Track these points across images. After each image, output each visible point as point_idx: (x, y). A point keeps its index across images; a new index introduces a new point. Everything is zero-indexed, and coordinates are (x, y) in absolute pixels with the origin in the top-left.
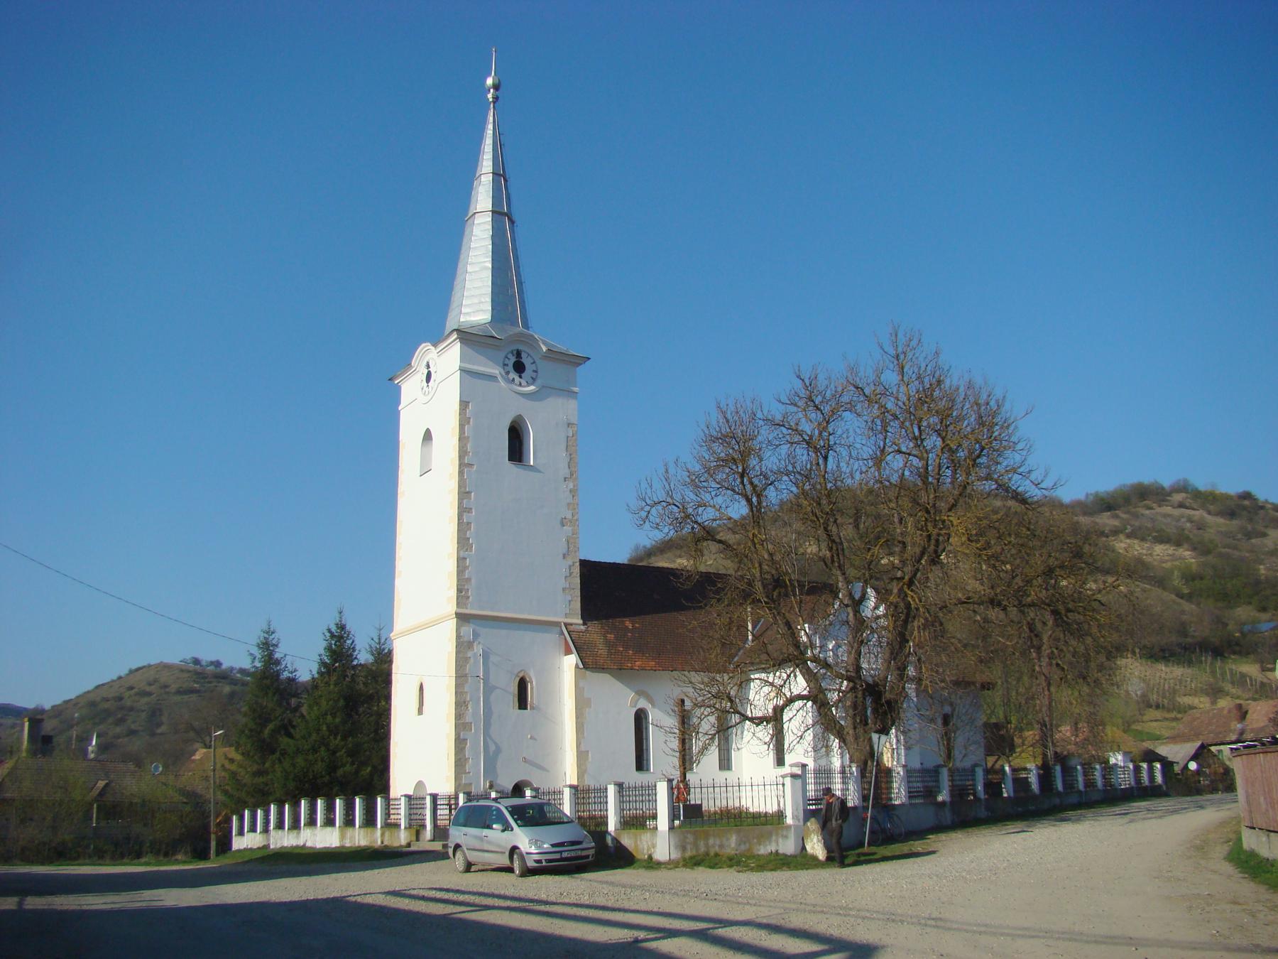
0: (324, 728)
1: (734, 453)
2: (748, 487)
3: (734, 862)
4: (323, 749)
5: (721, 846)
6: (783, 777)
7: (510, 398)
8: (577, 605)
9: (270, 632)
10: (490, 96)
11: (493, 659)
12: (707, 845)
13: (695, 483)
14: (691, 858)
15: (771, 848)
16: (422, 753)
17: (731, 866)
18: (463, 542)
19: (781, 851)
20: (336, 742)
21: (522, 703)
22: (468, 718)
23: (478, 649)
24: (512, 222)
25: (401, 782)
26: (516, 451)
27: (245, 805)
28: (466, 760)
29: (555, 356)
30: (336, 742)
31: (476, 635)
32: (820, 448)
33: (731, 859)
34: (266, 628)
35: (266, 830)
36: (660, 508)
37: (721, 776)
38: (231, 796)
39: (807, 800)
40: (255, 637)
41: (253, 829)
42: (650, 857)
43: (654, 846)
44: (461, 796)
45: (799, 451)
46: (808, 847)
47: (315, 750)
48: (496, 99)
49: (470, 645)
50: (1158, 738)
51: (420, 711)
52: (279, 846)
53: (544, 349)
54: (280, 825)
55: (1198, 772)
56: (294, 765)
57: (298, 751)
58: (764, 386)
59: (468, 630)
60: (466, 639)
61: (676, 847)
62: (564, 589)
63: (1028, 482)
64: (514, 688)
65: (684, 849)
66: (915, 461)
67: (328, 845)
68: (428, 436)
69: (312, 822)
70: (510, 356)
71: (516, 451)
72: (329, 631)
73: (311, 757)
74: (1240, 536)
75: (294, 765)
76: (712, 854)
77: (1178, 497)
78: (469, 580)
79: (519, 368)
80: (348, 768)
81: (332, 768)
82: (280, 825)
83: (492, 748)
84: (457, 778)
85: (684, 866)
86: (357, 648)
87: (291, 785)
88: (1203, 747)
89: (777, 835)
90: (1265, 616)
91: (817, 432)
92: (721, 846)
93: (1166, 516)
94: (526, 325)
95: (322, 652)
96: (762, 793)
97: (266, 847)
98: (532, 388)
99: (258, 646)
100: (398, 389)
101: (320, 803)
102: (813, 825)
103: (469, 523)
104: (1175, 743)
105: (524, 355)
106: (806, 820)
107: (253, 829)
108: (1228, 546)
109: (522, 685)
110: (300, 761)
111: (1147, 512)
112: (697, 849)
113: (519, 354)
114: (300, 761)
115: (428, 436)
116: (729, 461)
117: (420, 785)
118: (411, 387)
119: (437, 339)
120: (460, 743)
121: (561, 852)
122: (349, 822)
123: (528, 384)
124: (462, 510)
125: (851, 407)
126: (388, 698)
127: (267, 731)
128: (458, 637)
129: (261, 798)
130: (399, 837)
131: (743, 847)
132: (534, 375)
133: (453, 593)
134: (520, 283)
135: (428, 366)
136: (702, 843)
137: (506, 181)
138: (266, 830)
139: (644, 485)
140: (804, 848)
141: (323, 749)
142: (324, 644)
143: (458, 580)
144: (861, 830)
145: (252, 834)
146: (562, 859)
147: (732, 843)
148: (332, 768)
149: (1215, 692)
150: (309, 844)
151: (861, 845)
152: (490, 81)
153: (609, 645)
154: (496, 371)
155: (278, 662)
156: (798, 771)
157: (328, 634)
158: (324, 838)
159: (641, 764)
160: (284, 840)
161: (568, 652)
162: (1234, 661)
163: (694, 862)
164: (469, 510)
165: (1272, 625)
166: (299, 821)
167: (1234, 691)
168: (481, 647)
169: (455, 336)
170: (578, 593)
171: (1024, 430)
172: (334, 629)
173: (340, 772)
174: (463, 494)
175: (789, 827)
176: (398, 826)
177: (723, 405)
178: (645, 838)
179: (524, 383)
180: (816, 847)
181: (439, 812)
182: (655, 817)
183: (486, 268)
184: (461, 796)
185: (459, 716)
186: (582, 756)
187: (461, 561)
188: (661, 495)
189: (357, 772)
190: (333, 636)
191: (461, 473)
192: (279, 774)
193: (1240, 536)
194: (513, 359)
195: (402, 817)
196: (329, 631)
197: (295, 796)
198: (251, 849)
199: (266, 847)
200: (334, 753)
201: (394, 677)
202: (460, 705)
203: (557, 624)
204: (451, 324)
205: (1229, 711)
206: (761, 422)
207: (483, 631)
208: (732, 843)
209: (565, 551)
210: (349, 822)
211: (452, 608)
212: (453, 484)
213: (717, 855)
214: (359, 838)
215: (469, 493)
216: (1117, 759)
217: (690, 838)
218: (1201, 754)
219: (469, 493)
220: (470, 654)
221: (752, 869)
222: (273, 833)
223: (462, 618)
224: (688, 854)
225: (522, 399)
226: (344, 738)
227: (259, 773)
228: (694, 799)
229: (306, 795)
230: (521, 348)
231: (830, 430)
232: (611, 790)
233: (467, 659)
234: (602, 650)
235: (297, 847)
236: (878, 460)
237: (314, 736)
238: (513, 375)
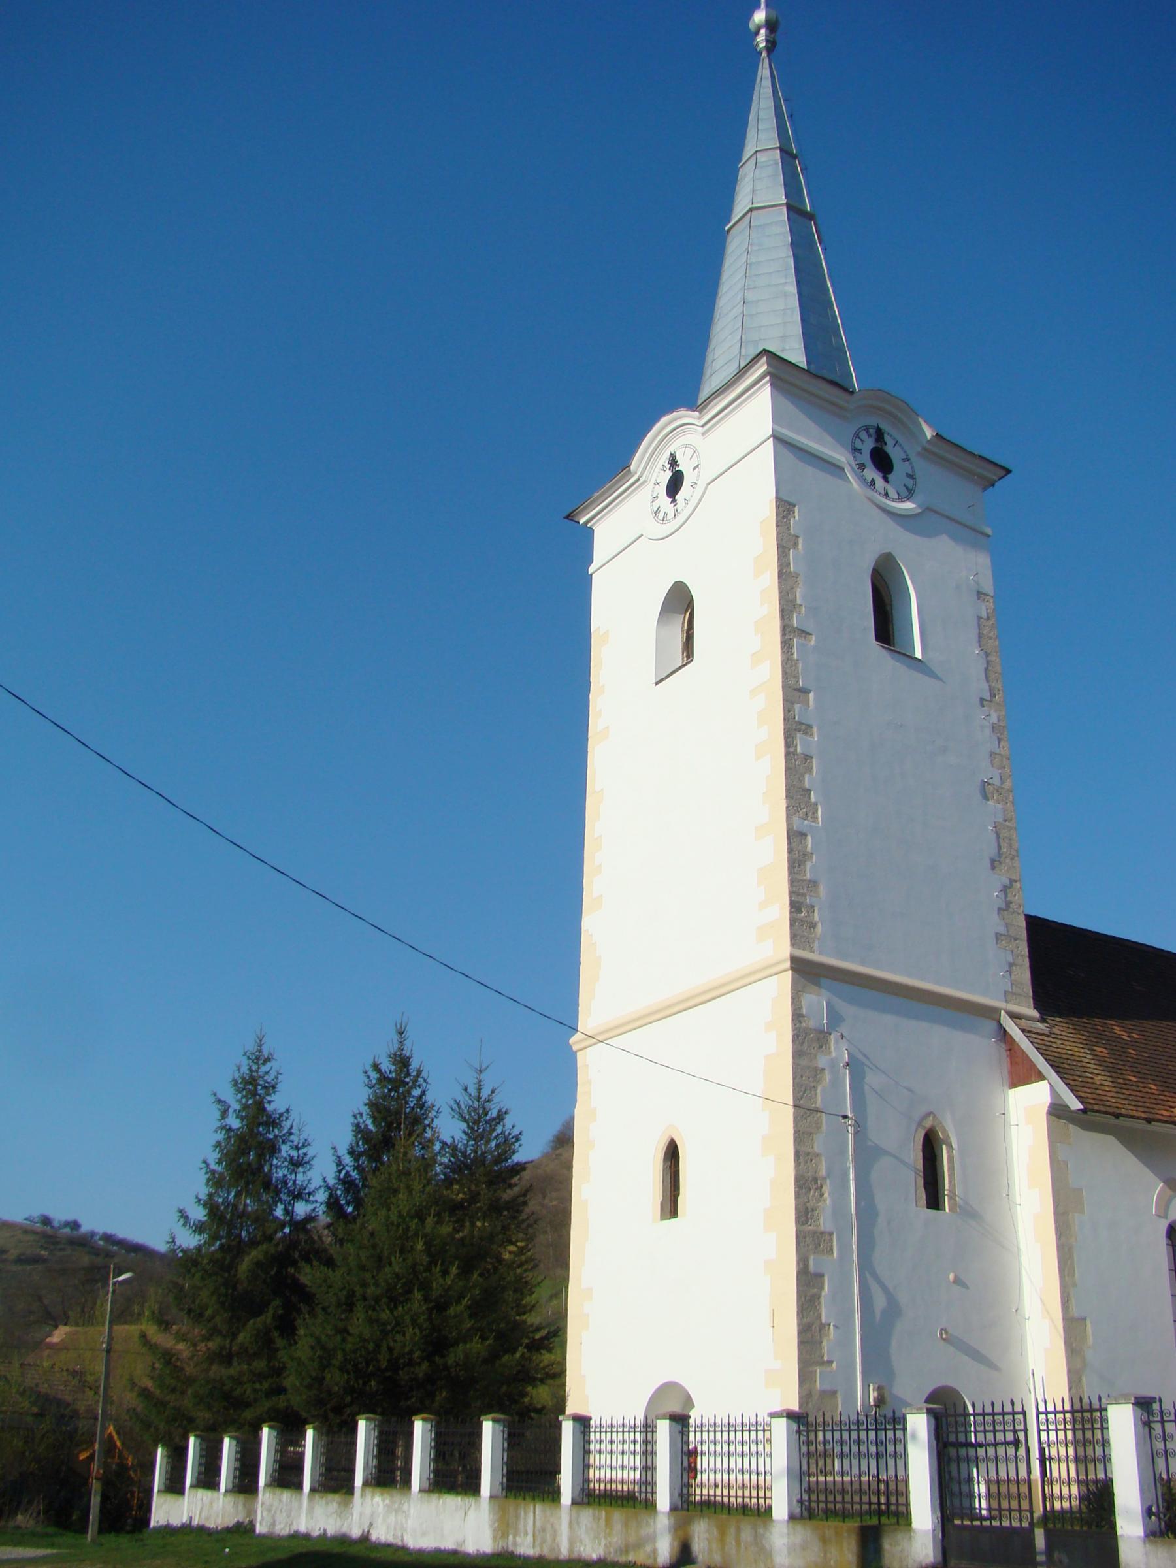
0: (420, 1246)
4: (417, 1295)
7: (869, 520)
8: (1024, 975)
11: (872, 1079)
22: (825, 1222)
23: (839, 1051)
26: (886, 626)
27: (187, 1424)
28: (823, 1327)
29: (947, 451)
30: (445, 1280)
31: (835, 1018)
34: (251, 1047)
35: (246, 1484)
38: (161, 1405)
40: (221, 1080)
41: (208, 1479)
44: (1122, 1423)
51: (671, 1206)
52: (282, 1529)
53: (929, 433)
59: (818, 1001)
60: (812, 1024)
62: (998, 936)
64: (915, 1156)
67: (448, 1544)
68: (679, 602)
70: (863, 435)
71: (886, 626)
72: (376, 1067)
73: (385, 1315)
78: (813, 884)
79: (882, 462)
80: (476, 1346)
81: (437, 1345)
83: (880, 1302)
84: (805, 1377)
87: (335, 1379)
95: (365, 1110)
97: (243, 1530)
98: (908, 506)
99: (235, 1083)
100: (588, 534)
103: (807, 757)
107: (208, 1479)
113: (879, 435)
114: (359, 1324)
115: (679, 602)
120: (808, 1283)
123: (901, 499)
127: (244, 1267)
129: (231, 1412)
133: (780, 911)
138: (246, 1484)
141: (417, 1295)
143: (792, 882)
145: (204, 1495)
148: (437, 1345)
150: (380, 1534)
153: (1099, 1060)
154: (842, 457)
155: (273, 1122)
157: (374, 1075)
161: (1022, 1074)
164: (807, 729)
168: (844, 1045)
169: (762, 367)
170: (1023, 948)
172: (387, 1066)
173: (456, 1356)
174: (794, 693)
176: (765, 1513)
179: (892, 493)
183: (786, 295)
184: (1122, 1423)
185: (804, 1215)
187: (795, 837)
190: (383, 1079)
191: (786, 646)
194: (869, 444)
196: (376, 1067)
197: (338, 1410)
198: (202, 1529)
199: (243, 1530)
200: (440, 1306)
203: (990, 1013)
207: (847, 1010)
209: (993, 851)
211: (779, 947)
212: (771, 671)
215: (805, 691)
219: (805, 691)
220: (822, 1061)
222: (265, 1495)
223: (806, 972)
225: (890, 523)
226: (466, 1271)
227: (225, 1357)
229: (368, 1409)
230: (884, 426)
233: (817, 1072)
235: (343, 1539)
238: (871, 473)
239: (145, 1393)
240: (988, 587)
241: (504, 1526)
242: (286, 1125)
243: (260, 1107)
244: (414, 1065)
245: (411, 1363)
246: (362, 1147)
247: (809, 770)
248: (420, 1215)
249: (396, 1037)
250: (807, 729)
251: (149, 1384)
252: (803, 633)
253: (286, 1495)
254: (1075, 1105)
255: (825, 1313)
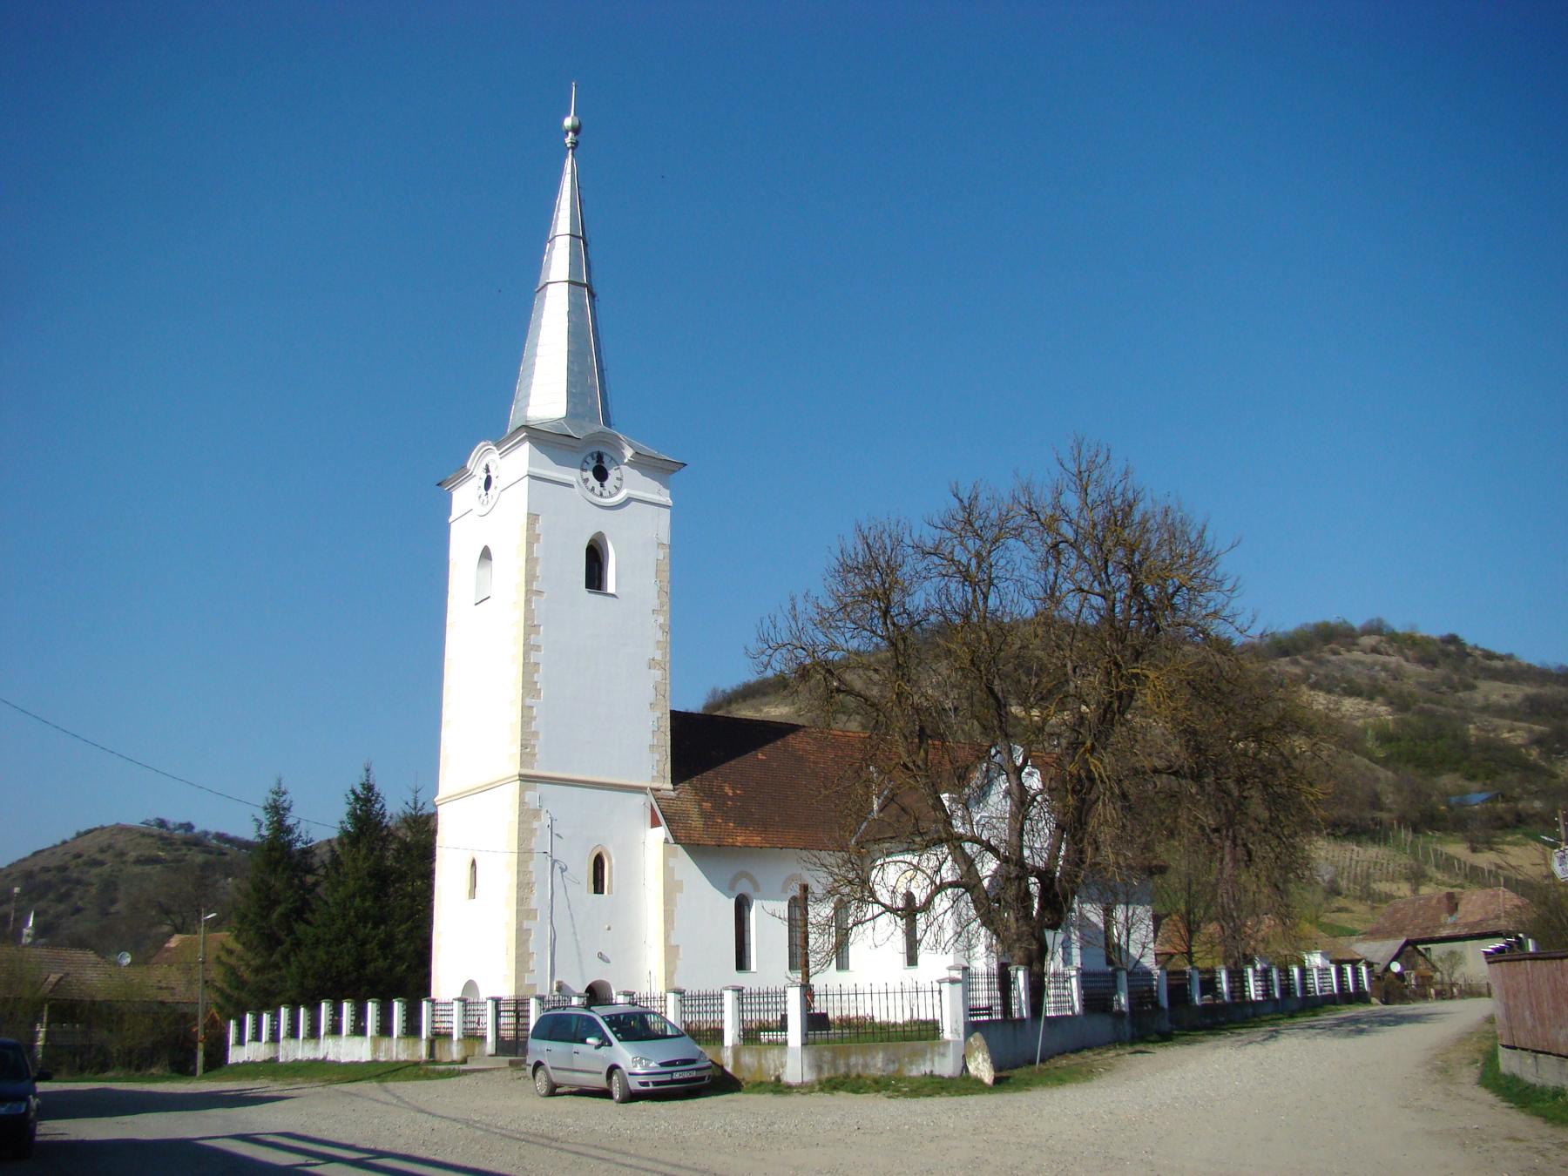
1: (874, 581)
2: (891, 628)
3: (883, 1085)
5: (865, 1066)
6: (940, 982)
9: (279, 793)
10: (568, 140)
12: (848, 1065)
13: (825, 621)
14: (829, 1080)
15: (925, 1068)
16: (475, 947)
17: (878, 1091)
18: (529, 687)
19: (936, 1072)
20: (364, 931)
21: (598, 886)
22: (533, 904)
24: (592, 295)
25: (445, 982)
32: (978, 578)
33: (876, 1081)
34: (274, 787)
35: (274, 1038)
36: (784, 651)
37: (845, 980)
38: (228, 998)
39: (973, 1010)
42: (778, 1079)
43: (783, 1066)
45: (953, 586)
46: (971, 1068)
47: (340, 940)
48: (575, 145)
49: (536, 814)
50: (1352, 933)
52: (291, 1059)
54: (293, 1033)
55: (1400, 976)
56: (313, 958)
57: (318, 942)
58: (911, 503)
59: (535, 793)
61: (810, 1067)
63: (1232, 629)
65: (820, 1069)
66: (1097, 601)
67: (356, 1059)
68: (486, 554)
69: (335, 1029)
70: (589, 459)
72: (354, 792)
73: (333, 949)
74: (1444, 689)
75: (313, 958)
76: (854, 1075)
77: (1368, 641)
80: (381, 963)
81: (361, 963)
82: (293, 1033)
85: (822, 1090)
86: (388, 814)
88: (1407, 943)
89: (933, 1052)
90: (1475, 785)
91: (974, 562)
92: (865, 1066)
93: (1356, 662)
94: (607, 423)
95: (345, 818)
96: (899, 1003)
97: (274, 1060)
101: (347, 1007)
102: (977, 1039)
103: (537, 664)
104: (1375, 939)
105: (606, 459)
106: (968, 1034)
107: (257, 1037)
108: (1432, 701)
109: (598, 863)
110: (321, 954)
111: (1333, 658)
112: (836, 1070)
113: (600, 457)
114: (321, 954)
115: (486, 554)
116: (868, 595)
117: (470, 986)
118: (465, 496)
119: (501, 438)
121: (671, 1073)
122: (385, 1029)
124: (529, 648)
125: (1018, 533)
126: (428, 876)
128: (522, 803)
129: (266, 1001)
130: (451, 1053)
131: (892, 1068)
132: (618, 483)
133: (517, 749)
134: (601, 371)
135: (487, 470)
136: (841, 1062)
137: (586, 245)
138: (274, 1038)
139: (767, 623)
140: (965, 1067)
142: (347, 808)
144: (1022, 1047)
146: (673, 1082)
147: (878, 1062)
148: (361, 963)
149: (1416, 877)
150: (331, 1057)
151: (1032, 1062)
152: (568, 122)
153: (704, 814)
155: (289, 830)
156: (958, 975)
158: (352, 1049)
159: (742, 963)
160: (297, 1051)
161: (655, 823)
162: (1440, 840)
163: (832, 1085)
165: (1483, 796)
166: (318, 1028)
167: (1439, 875)
171: (1226, 566)
172: (359, 790)
173: (370, 969)
174: (531, 627)
175: (948, 1042)
176: (450, 1035)
177: (865, 527)
178: (772, 1055)
179: (605, 493)
180: (981, 1067)
181: (502, 1020)
182: (783, 1025)
185: (522, 901)
186: (671, 952)
187: (526, 710)
188: (785, 636)
189: (391, 968)
190: (357, 798)
191: (528, 602)
192: (294, 969)
193: (1444, 689)
194: (593, 464)
195: (455, 1025)
196: (354, 792)
197: (313, 998)
198: (254, 1063)
199: (274, 1060)
200: (364, 943)
201: (439, 852)
202: (524, 887)
204: (514, 421)
205: (1439, 901)
206: (910, 551)
208: (878, 1062)
209: (652, 699)
210: (385, 1029)
211: (515, 768)
213: (859, 1076)
214: (397, 1049)
216: (1315, 960)
217: (828, 1055)
218: (1407, 952)
220: (536, 825)
221: (905, 1095)
224: (825, 1075)
228: (819, 1006)
229: (325, 997)
231: (992, 560)
232: (729, 997)
234: (697, 822)
236: (1052, 594)
237: (339, 923)
239: (220, 991)
240: (666, 540)
241: (375, 1048)
242: (297, 832)
243: (281, 822)
244: (376, 789)
245: (347, 973)
246: (346, 841)
247: (537, 671)
248: (354, 896)
249: (364, 774)
250: (537, 648)
251: (225, 986)
252: (539, 593)
253: (292, 1042)
254: (671, 840)
255: (532, 947)
